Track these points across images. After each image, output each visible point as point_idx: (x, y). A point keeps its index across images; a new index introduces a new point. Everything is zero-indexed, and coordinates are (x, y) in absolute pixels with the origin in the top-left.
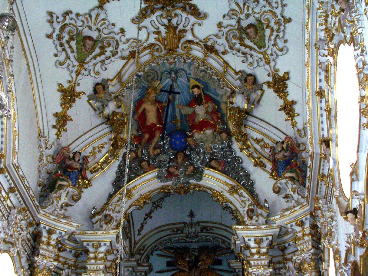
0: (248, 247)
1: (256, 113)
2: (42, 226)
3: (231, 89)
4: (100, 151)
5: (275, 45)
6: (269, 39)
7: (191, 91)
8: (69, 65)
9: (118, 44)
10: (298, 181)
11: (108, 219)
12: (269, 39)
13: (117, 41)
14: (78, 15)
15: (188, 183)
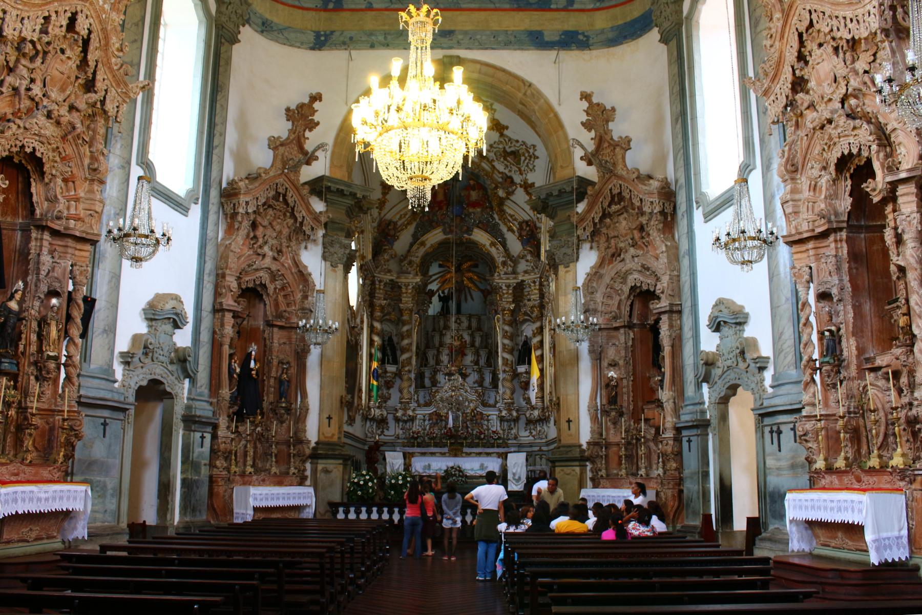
5: (527, 166)
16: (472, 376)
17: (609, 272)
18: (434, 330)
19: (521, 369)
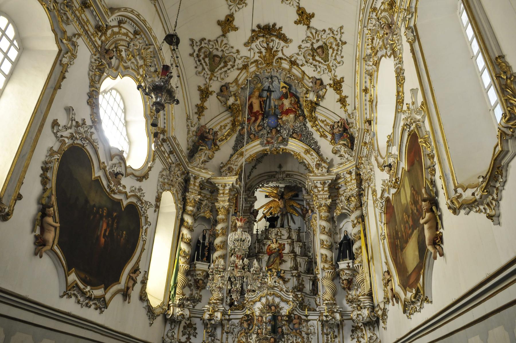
0: (316, 187)
1: (321, 104)
2: (190, 174)
3: (306, 89)
4: (225, 128)
6: (332, 56)
7: (281, 90)
8: (204, 74)
9: (235, 60)
10: (348, 146)
11: (230, 170)
12: (332, 56)
13: (234, 58)
14: (209, 41)
15: (279, 147)
19: (343, 265)
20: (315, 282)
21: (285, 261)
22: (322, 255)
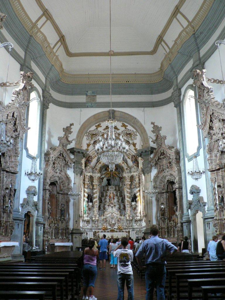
0: (126, 177)
14: (92, 131)
16: (117, 206)
17: (161, 176)
18: (104, 191)
19: (133, 203)
20: (124, 206)
21: (115, 199)
22: (127, 200)
